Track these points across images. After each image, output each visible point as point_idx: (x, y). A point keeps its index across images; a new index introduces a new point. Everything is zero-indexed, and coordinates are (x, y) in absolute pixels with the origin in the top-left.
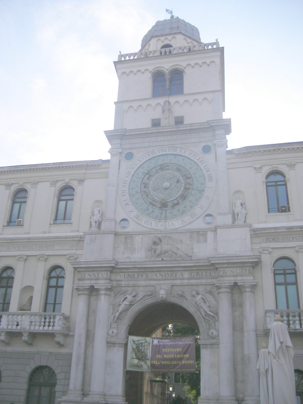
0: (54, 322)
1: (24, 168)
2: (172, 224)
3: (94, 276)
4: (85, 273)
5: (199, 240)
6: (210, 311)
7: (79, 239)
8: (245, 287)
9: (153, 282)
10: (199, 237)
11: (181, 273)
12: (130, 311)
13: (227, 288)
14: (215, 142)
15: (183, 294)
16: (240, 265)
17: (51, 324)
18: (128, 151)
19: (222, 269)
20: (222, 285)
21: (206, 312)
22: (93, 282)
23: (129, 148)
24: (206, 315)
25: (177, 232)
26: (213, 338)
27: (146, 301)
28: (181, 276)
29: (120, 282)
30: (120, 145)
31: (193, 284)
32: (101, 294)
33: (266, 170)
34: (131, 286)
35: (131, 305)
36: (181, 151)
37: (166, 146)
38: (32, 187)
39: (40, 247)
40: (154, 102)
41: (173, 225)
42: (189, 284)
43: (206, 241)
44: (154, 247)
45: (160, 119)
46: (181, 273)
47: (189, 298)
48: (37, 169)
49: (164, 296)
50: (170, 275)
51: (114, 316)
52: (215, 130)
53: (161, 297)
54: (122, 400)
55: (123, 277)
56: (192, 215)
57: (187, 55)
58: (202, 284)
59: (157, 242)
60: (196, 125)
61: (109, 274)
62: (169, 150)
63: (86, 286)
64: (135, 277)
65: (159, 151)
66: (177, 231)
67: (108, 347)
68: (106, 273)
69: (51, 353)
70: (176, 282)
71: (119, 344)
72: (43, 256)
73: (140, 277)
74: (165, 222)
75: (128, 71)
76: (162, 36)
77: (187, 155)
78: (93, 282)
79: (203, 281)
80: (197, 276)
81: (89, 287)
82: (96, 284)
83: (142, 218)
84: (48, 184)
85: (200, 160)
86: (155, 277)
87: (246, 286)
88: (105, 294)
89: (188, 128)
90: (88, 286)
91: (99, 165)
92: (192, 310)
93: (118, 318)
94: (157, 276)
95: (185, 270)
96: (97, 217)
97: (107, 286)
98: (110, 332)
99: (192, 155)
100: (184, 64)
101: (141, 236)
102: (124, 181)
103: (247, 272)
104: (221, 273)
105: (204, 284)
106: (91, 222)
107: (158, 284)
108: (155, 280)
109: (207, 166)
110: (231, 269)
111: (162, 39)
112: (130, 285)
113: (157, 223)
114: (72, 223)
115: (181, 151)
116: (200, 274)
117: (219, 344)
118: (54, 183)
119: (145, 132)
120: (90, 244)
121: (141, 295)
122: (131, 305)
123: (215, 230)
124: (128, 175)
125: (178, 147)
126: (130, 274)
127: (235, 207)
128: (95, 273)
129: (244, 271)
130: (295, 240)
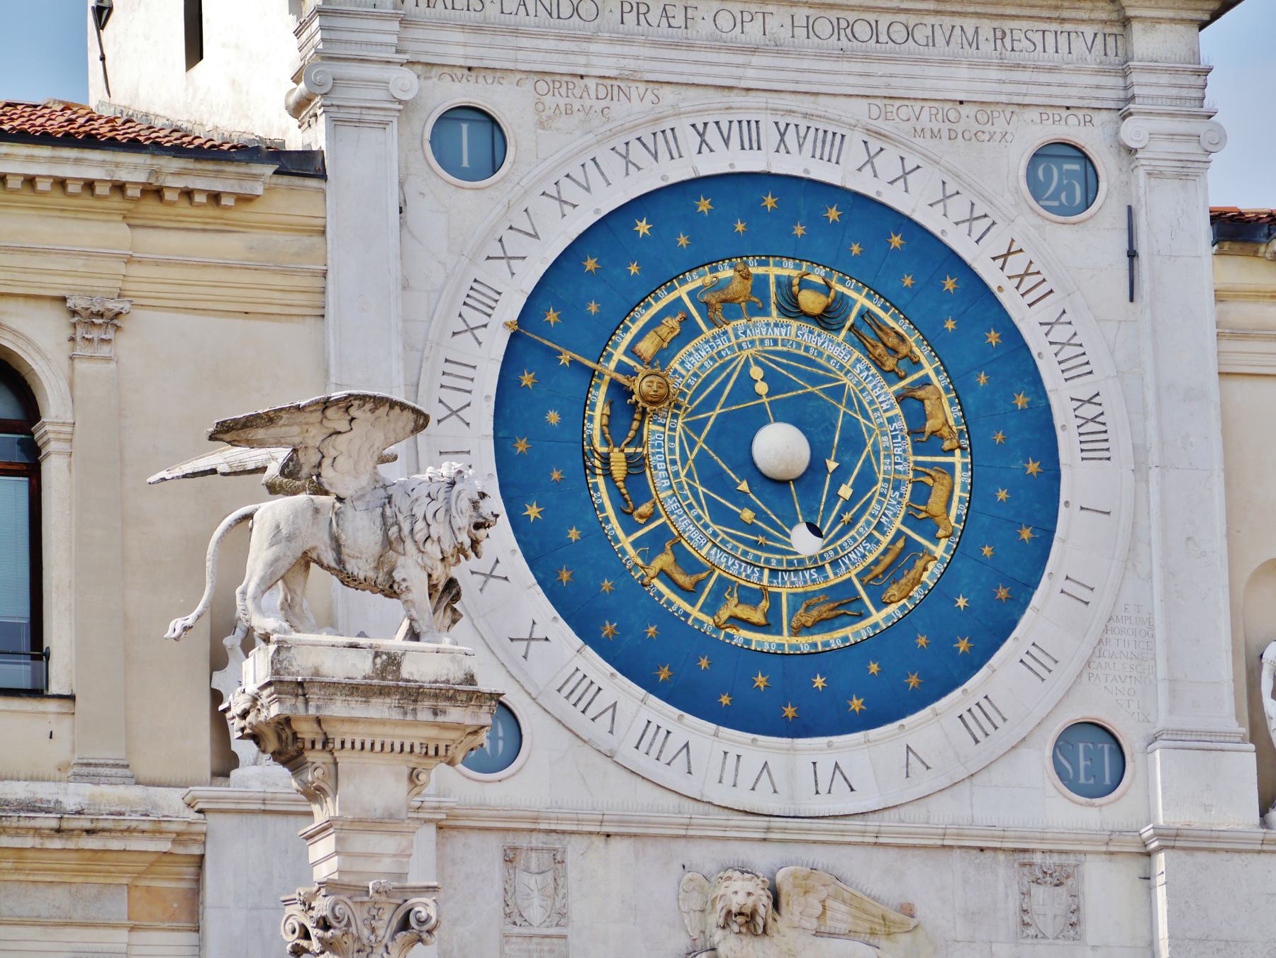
2: (837, 772)
5: (1027, 919)
7: (166, 846)
14: (1132, 131)
23: (461, 62)
30: (395, 26)
36: (870, 160)
41: (842, 773)
43: (1073, 923)
52: (1126, 22)
56: (975, 718)
59: (762, 910)
62: (782, 135)
65: (701, 135)
83: (614, 705)
85: (1016, 264)
99: (958, 208)
102: (450, 368)
109: (1070, 330)
113: (731, 759)
114: (71, 698)
115: (870, 160)
124: (475, 318)
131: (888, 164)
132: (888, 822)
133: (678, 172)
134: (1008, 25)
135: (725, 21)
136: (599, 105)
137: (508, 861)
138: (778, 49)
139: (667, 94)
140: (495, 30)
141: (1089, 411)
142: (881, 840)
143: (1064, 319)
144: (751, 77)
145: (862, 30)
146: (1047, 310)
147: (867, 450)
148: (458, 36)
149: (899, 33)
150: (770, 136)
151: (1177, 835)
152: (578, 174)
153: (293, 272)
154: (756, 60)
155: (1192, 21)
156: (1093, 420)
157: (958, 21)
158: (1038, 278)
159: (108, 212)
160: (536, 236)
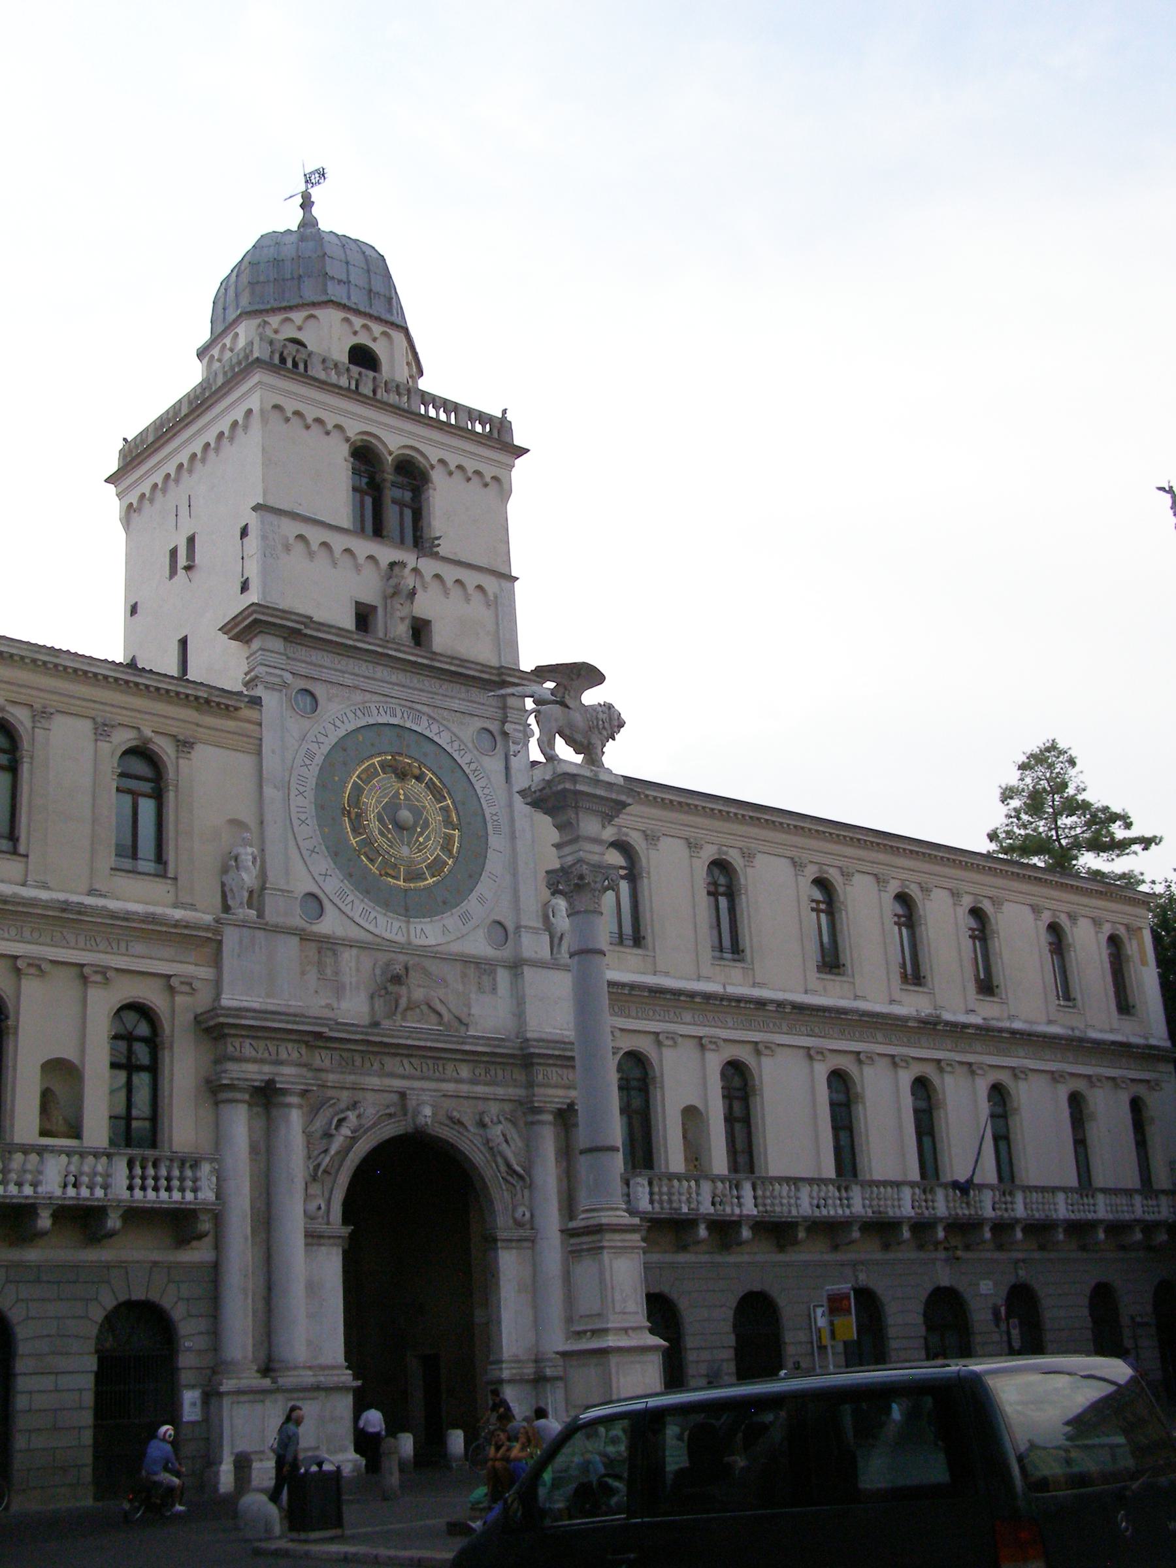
0: (195, 1180)
1: (14, 651)
3: (266, 1055)
4: (241, 1040)
7: (210, 935)
9: (398, 1083)
10: (479, 977)
18: (302, 684)
19: (541, 1068)
21: (508, 1165)
26: (519, 1224)
27: (385, 1129)
28: (455, 1074)
29: (323, 1075)
31: (478, 1095)
32: (289, 1105)
34: (348, 1088)
35: (351, 1138)
37: (393, 700)
38: (39, 725)
39: (88, 938)
40: (364, 547)
43: (494, 989)
44: (391, 988)
45: (374, 608)
47: (472, 1130)
48: (56, 666)
49: (429, 1121)
50: (431, 1066)
51: (316, 1163)
53: (423, 1123)
54: (351, 1378)
55: (327, 1063)
60: (473, 666)
61: (303, 1050)
68: (296, 1045)
69: (155, 1264)
70: (445, 1086)
71: (330, 1237)
72: (103, 971)
74: (408, 922)
75: (290, 406)
76: (358, 312)
77: (443, 740)
78: (267, 1068)
79: (500, 1091)
81: (263, 1085)
82: (277, 1074)
84: (87, 725)
85: (473, 766)
86: (400, 1071)
88: (300, 1106)
89: (453, 668)
90: (262, 1081)
91: (237, 709)
92: (479, 1157)
93: (325, 1171)
95: (465, 1061)
96: (249, 878)
98: (312, 1206)
99: (456, 745)
100: (434, 454)
101: (354, 951)
104: (540, 1077)
106: (223, 885)
108: (403, 1077)
110: (559, 1071)
111: (358, 322)
112: (348, 1086)
116: (492, 1072)
117: (533, 1241)
118: (102, 730)
119: (351, 643)
120: (239, 956)
122: (353, 1140)
123: (516, 966)
124: (308, 762)
125: (424, 714)
126: (345, 1054)
128: (268, 1043)
130: (658, 1018)
133: (372, 721)
135: (385, 673)
136: (347, 695)
137: (319, 952)
139: (368, 696)
140: (315, 665)
141: (495, 818)
146: (483, 783)
148: (303, 665)
149: (437, 685)
150: (399, 714)
152: (340, 717)
153: (250, 737)
154: (396, 688)
159: (192, 707)
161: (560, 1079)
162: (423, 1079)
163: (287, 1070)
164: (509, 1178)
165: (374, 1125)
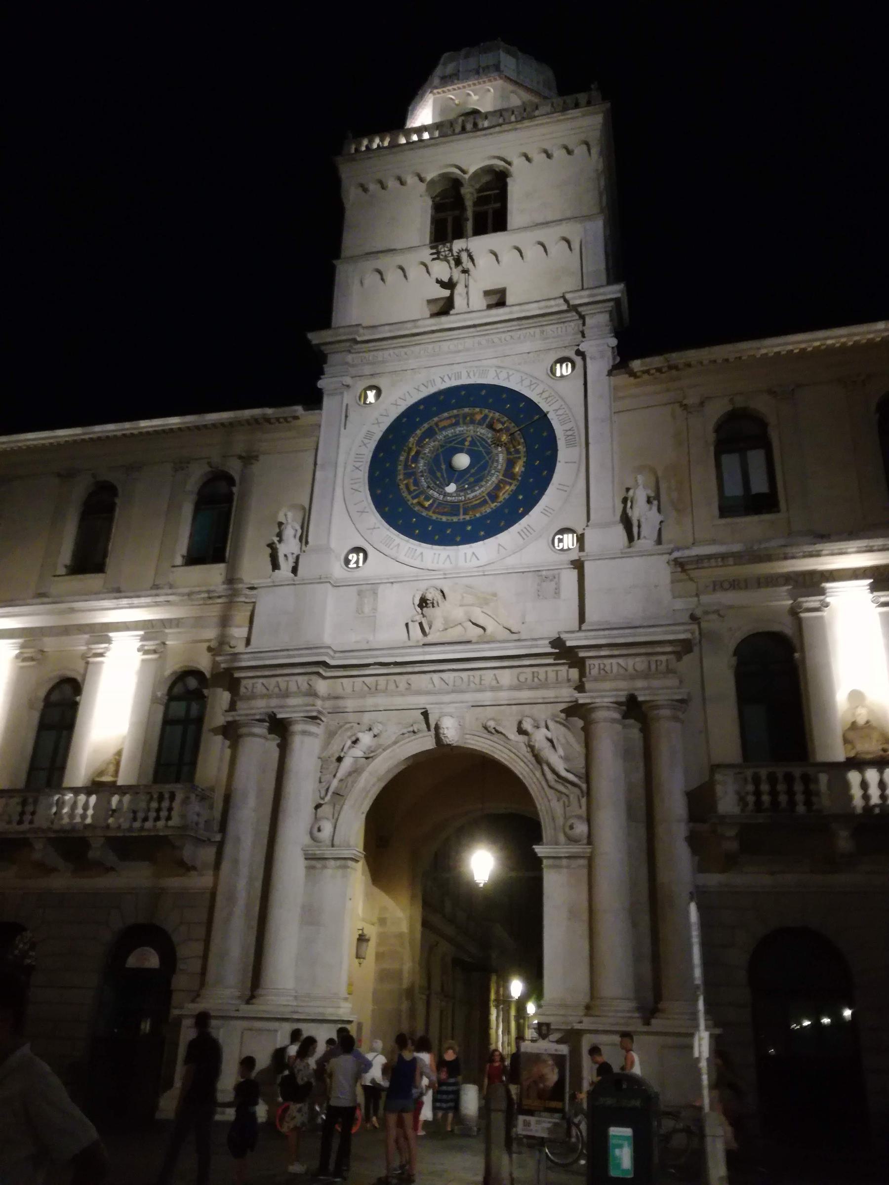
0: (170, 809)
3: (277, 690)
6: (567, 771)
8: (657, 707)
11: (495, 675)
12: (365, 775)
13: (608, 708)
15: (500, 729)
16: (643, 650)
17: (164, 814)
20: (595, 703)
22: (274, 702)
24: (556, 781)
25: (484, 575)
28: (494, 683)
29: (341, 703)
33: (717, 410)
42: (513, 702)
43: (557, 592)
46: (495, 675)
57: (516, 129)
58: (546, 701)
59: (435, 599)
63: (255, 714)
64: (379, 687)
66: (484, 571)
67: (310, 868)
73: (392, 686)
78: (274, 702)
80: (533, 681)
82: (282, 707)
85: (545, 395)
86: (430, 686)
87: (659, 703)
92: (522, 768)
94: (434, 685)
97: (307, 711)
103: (663, 667)
105: (552, 700)
107: (436, 704)
108: (428, 693)
113: (437, 556)
121: (391, 732)
127: (631, 507)
129: (653, 667)
131: (503, 375)
132: (486, 568)
134: (545, 328)
137: (359, 595)
138: (468, 350)
142: (486, 573)
143: (562, 407)
144: (458, 360)
145: (496, 340)
147: (483, 452)
150: (464, 374)
151: (587, 556)
154: (461, 354)
155: (606, 311)
156: (571, 435)
157: (528, 331)
158: (553, 397)
160: (388, 416)
161: (622, 671)
162: (453, 692)
163: (292, 701)
164: (561, 788)
165: (395, 743)
